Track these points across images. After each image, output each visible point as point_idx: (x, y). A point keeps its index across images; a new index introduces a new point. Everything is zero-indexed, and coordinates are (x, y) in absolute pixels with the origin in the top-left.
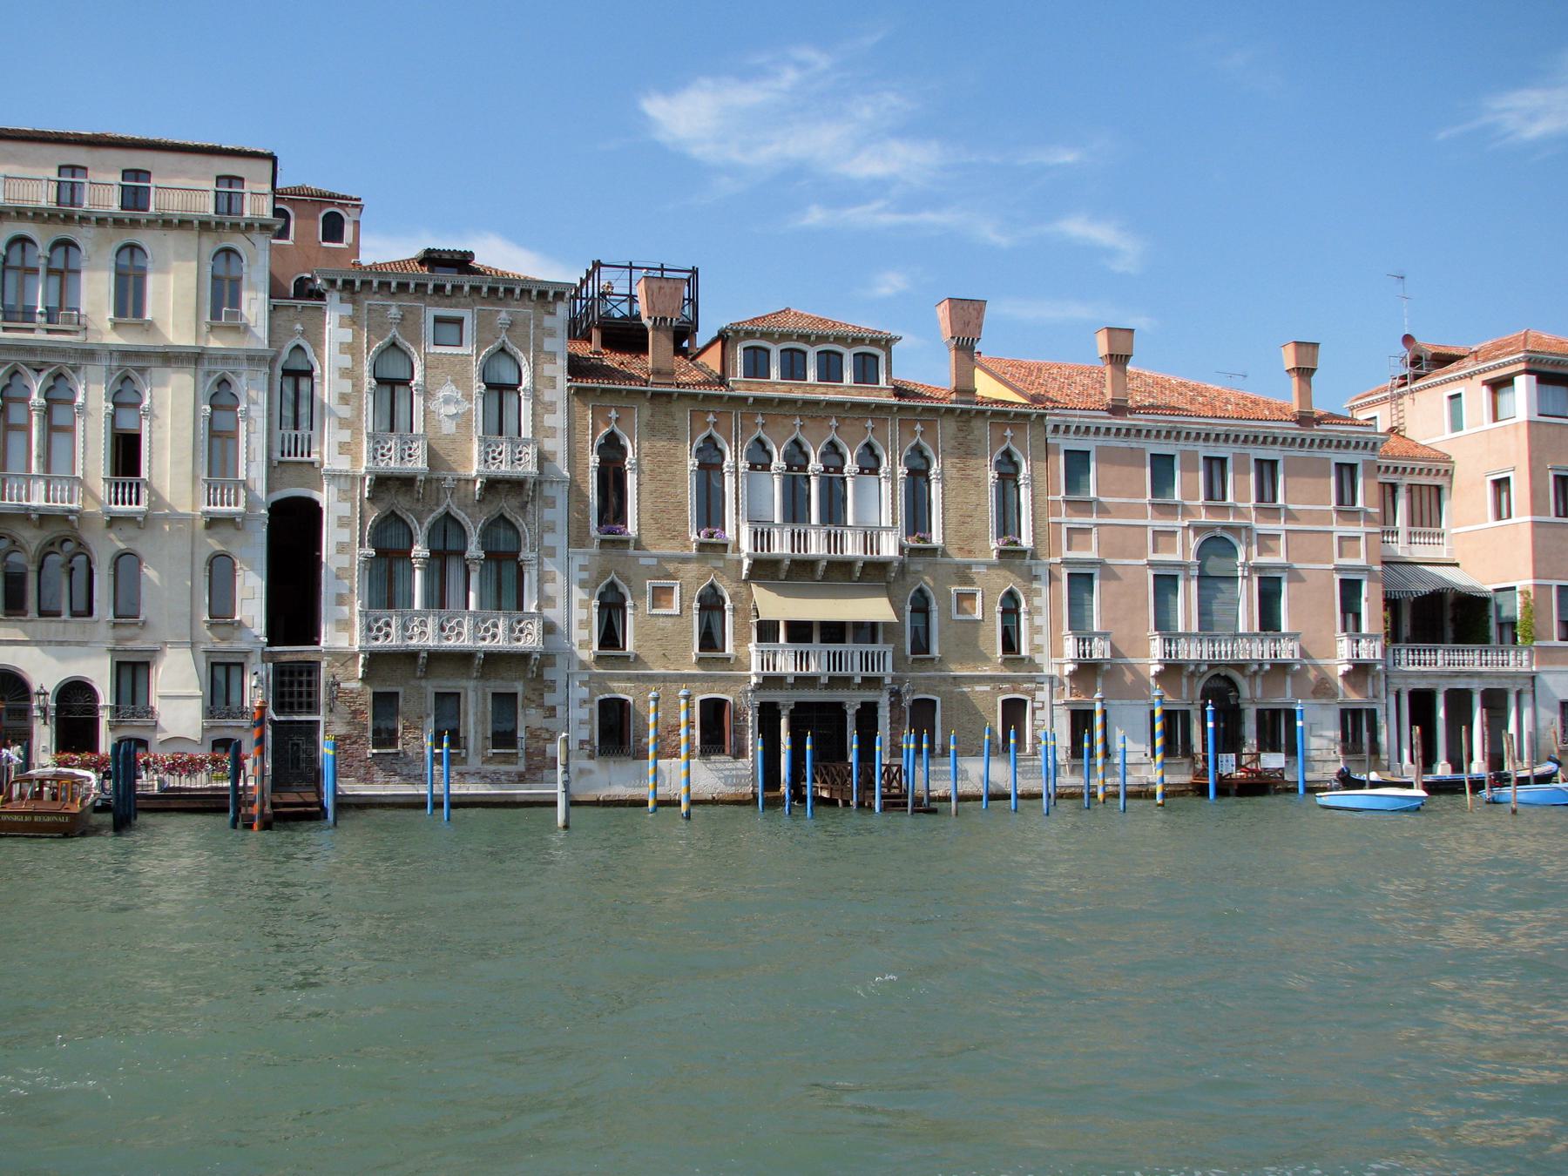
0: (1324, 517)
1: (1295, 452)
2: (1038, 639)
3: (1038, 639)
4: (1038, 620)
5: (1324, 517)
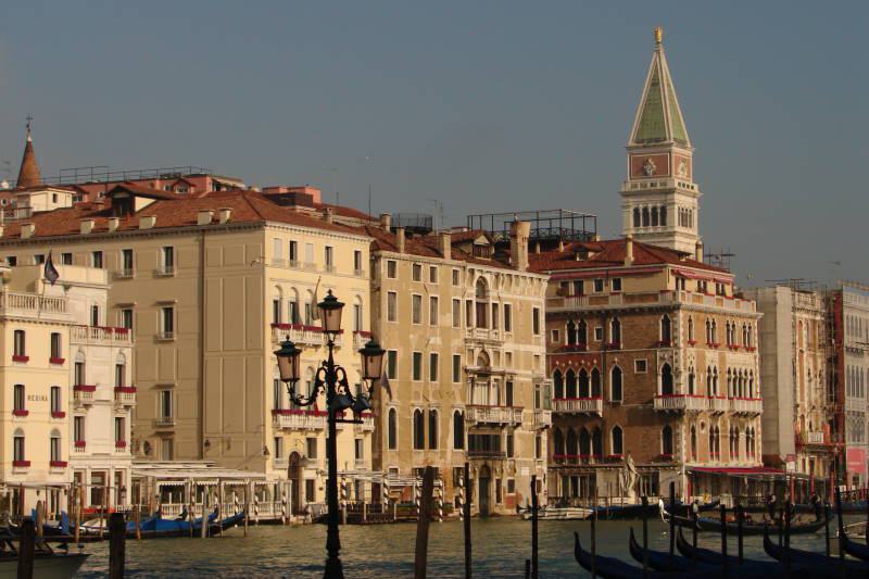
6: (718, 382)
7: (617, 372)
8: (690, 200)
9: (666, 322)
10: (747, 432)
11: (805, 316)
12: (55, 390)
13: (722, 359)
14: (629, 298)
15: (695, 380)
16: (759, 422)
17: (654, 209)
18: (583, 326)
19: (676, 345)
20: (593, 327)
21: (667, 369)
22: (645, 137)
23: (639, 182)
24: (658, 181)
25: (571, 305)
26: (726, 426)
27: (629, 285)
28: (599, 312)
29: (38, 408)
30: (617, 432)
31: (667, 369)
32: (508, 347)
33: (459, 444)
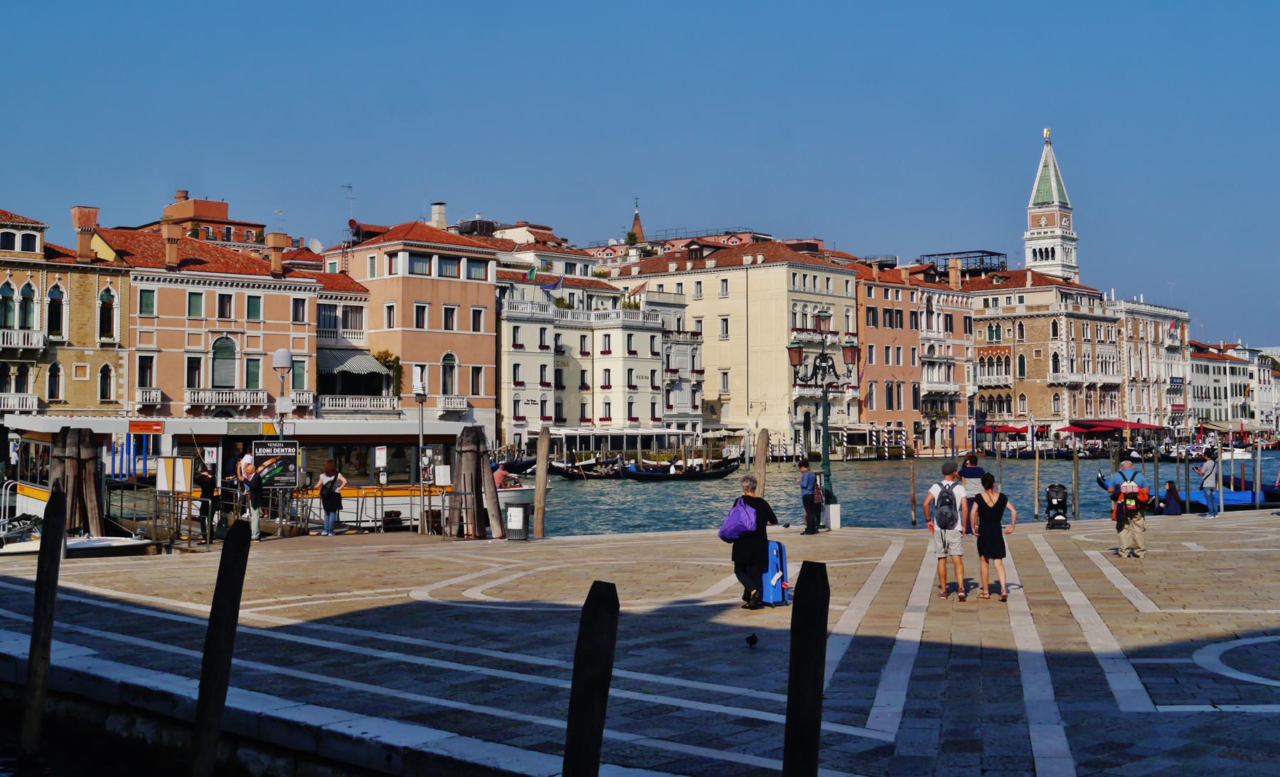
0: (286, 328)
1: (271, 292)
2: (121, 391)
3: (121, 391)
4: (121, 381)
5: (286, 328)
7: (1022, 359)
9: (1055, 325)
12: (653, 372)
13: (1094, 350)
14: (1030, 308)
18: (998, 326)
20: (1005, 326)
21: (1056, 356)
25: (990, 313)
27: (1031, 299)
29: (644, 385)
30: (1022, 397)
31: (1056, 356)
32: (949, 342)
33: (915, 407)
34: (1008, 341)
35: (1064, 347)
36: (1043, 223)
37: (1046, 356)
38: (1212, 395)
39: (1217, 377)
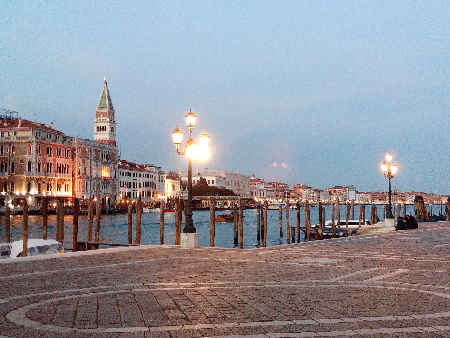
6: (52, 168)
8: (114, 125)
10: (65, 185)
11: (93, 148)
13: (55, 160)
14: (18, 138)
15: (41, 167)
16: (71, 182)
17: (103, 127)
19: (33, 155)
21: (30, 163)
22: (101, 107)
23: (99, 119)
24: (104, 119)
26: (55, 183)
28: (8, 143)
31: (30, 163)
34: (7, 155)
35: (34, 159)
36: (102, 116)
37: (25, 163)
38: (132, 186)
39: (135, 178)
